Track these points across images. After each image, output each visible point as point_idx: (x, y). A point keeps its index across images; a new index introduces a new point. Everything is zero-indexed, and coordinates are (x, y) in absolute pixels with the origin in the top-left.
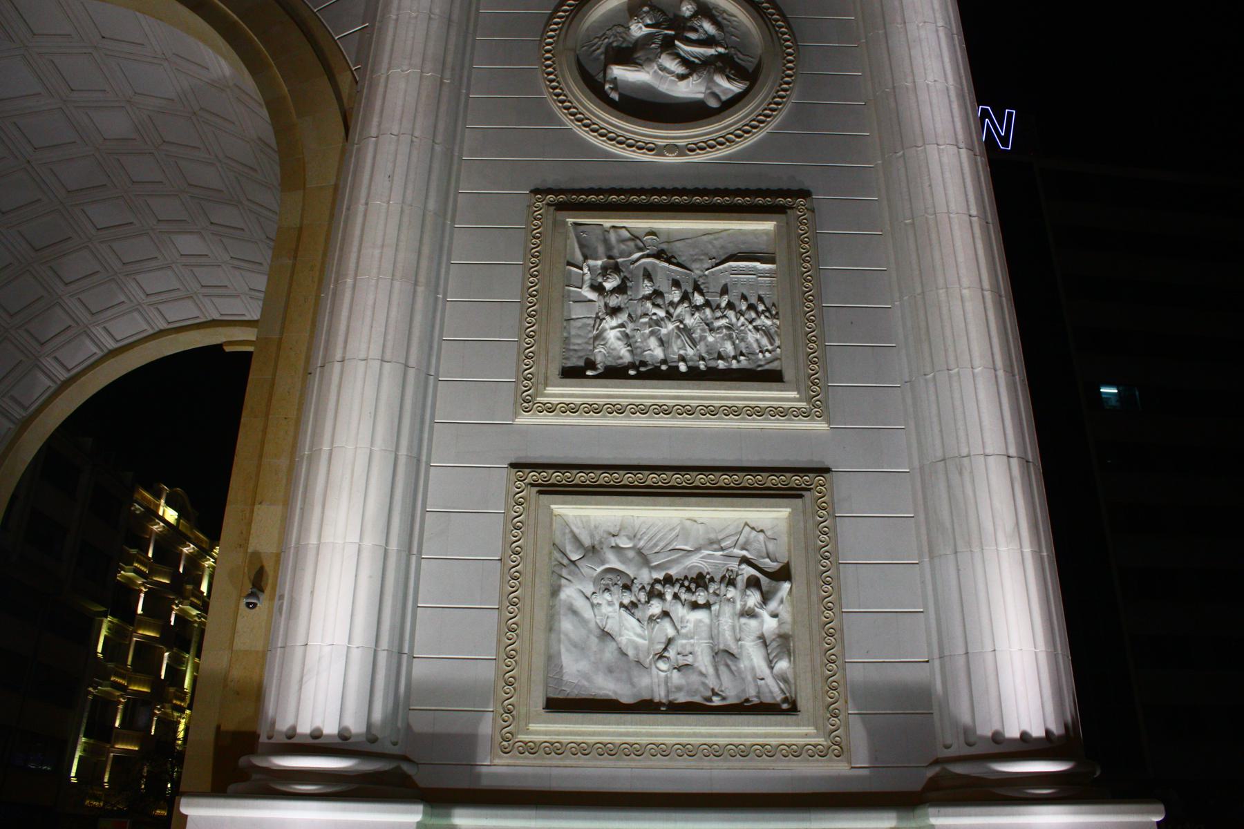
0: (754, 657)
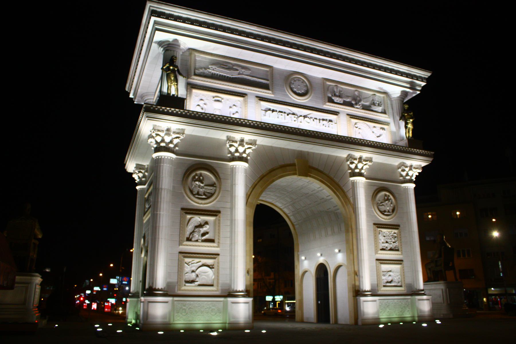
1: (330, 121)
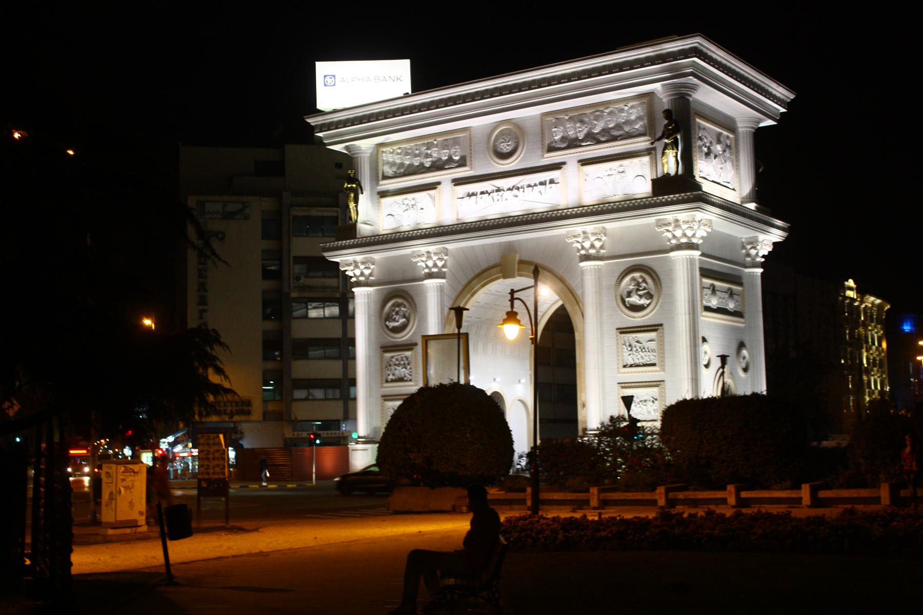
0: (653, 412)
1: (552, 182)
